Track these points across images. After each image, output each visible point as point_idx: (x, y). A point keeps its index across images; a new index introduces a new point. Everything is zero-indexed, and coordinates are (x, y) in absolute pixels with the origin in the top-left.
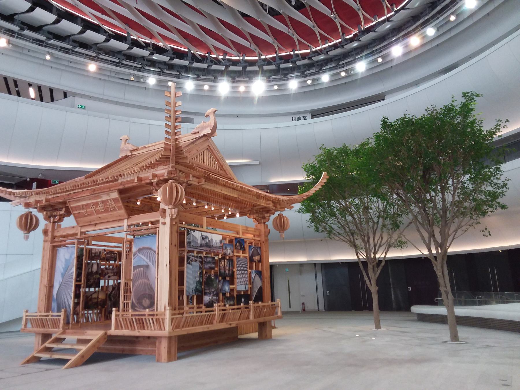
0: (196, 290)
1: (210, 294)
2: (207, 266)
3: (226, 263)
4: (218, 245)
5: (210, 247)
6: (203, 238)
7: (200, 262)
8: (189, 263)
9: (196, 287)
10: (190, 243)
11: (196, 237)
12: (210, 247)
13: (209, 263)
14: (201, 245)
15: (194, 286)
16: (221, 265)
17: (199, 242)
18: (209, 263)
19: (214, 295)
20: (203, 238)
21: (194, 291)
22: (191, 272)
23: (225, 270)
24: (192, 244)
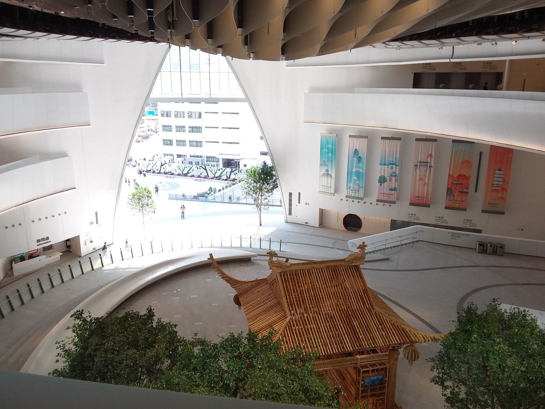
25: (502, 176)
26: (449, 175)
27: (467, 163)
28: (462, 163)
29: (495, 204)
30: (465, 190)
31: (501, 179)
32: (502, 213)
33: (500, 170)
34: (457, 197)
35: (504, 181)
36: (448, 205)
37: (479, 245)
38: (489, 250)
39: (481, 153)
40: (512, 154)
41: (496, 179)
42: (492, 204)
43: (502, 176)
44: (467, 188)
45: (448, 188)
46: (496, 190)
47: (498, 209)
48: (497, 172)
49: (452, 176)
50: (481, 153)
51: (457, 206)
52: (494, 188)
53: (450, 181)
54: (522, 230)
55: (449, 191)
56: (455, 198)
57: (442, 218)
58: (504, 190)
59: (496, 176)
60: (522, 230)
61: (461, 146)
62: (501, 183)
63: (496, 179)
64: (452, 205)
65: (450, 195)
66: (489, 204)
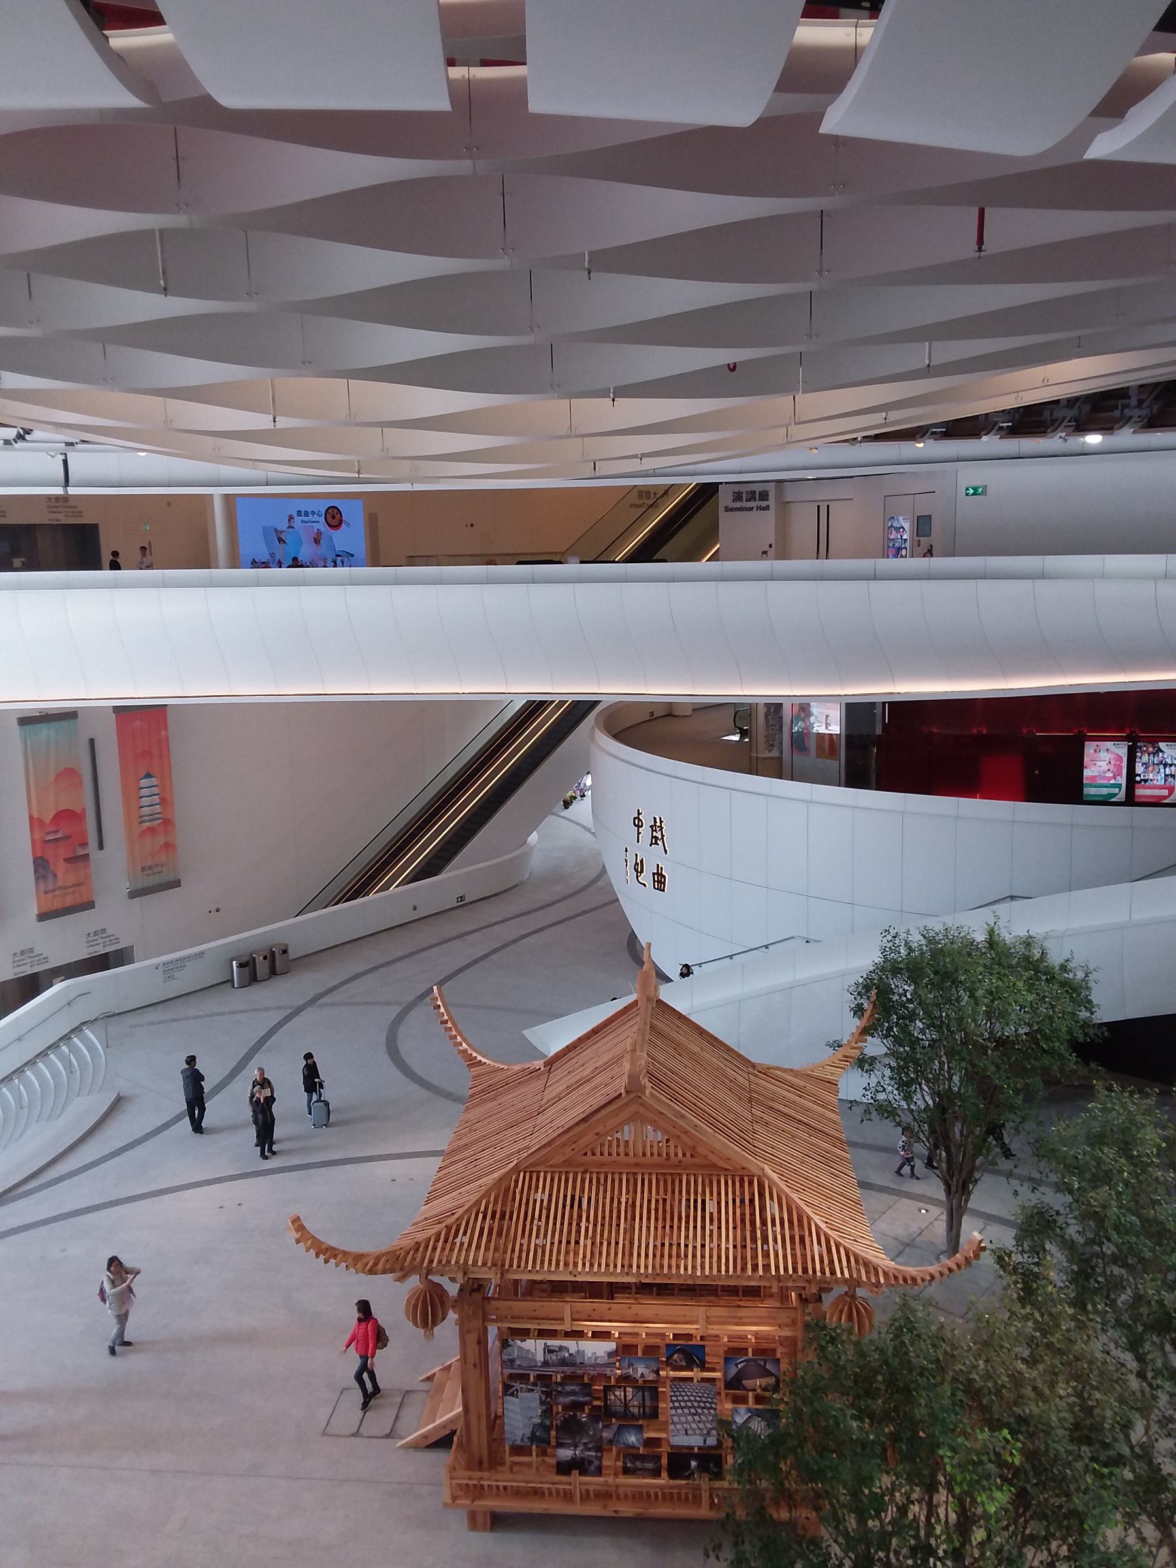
0: (533, 1438)
1: (576, 1446)
2: (568, 1400)
3: (630, 1395)
4: (606, 1360)
5: (574, 1365)
6: (551, 1351)
7: (542, 1392)
8: (512, 1395)
9: (533, 1433)
10: (512, 1361)
11: (528, 1351)
12: (574, 1365)
13: (573, 1393)
14: (545, 1363)
15: (528, 1432)
16: (612, 1397)
17: (540, 1358)
18: (573, 1393)
19: (589, 1450)
20: (548, 1350)
21: (526, 1440)
22: (518, 1409)
23: (626, 1405)
24: (518, 1362)
25: (156, 790)
26: (31, 818)
27: (69, 774)
28: (58, 776)
29: (157, 866)
30: (81, 852)
31: (156, 799)
32: (176, 884)
33: (148, 776)
34: (64, 874)
35: (163, 801)
36: (44, 910)
37: (241, 966)
38: (262, 968)
39: (92, 741)
40: (166, 729)
41: (145, 801)
42: (150, 867)
43: (156, 790)
44: (84, 844)
45: (35, 860)
46: (151, 830)
47: (166, 877)
48: (144, 782)
49: (40, 821)
50: (92, 741)
51: (69, 901)
52: (147, 824)
53: (37, 836)
54: (218, 910)
55: (41, 865)
56: (60, 883)
57: (31, 950)
58: (167, 822)
59: (144, 792)
60: (218, 910)
61: (45, 732)
62: (158, 808)
63: (145, 801)
64: (57, 904)
65: (44, 877)
66: (143, 869)
